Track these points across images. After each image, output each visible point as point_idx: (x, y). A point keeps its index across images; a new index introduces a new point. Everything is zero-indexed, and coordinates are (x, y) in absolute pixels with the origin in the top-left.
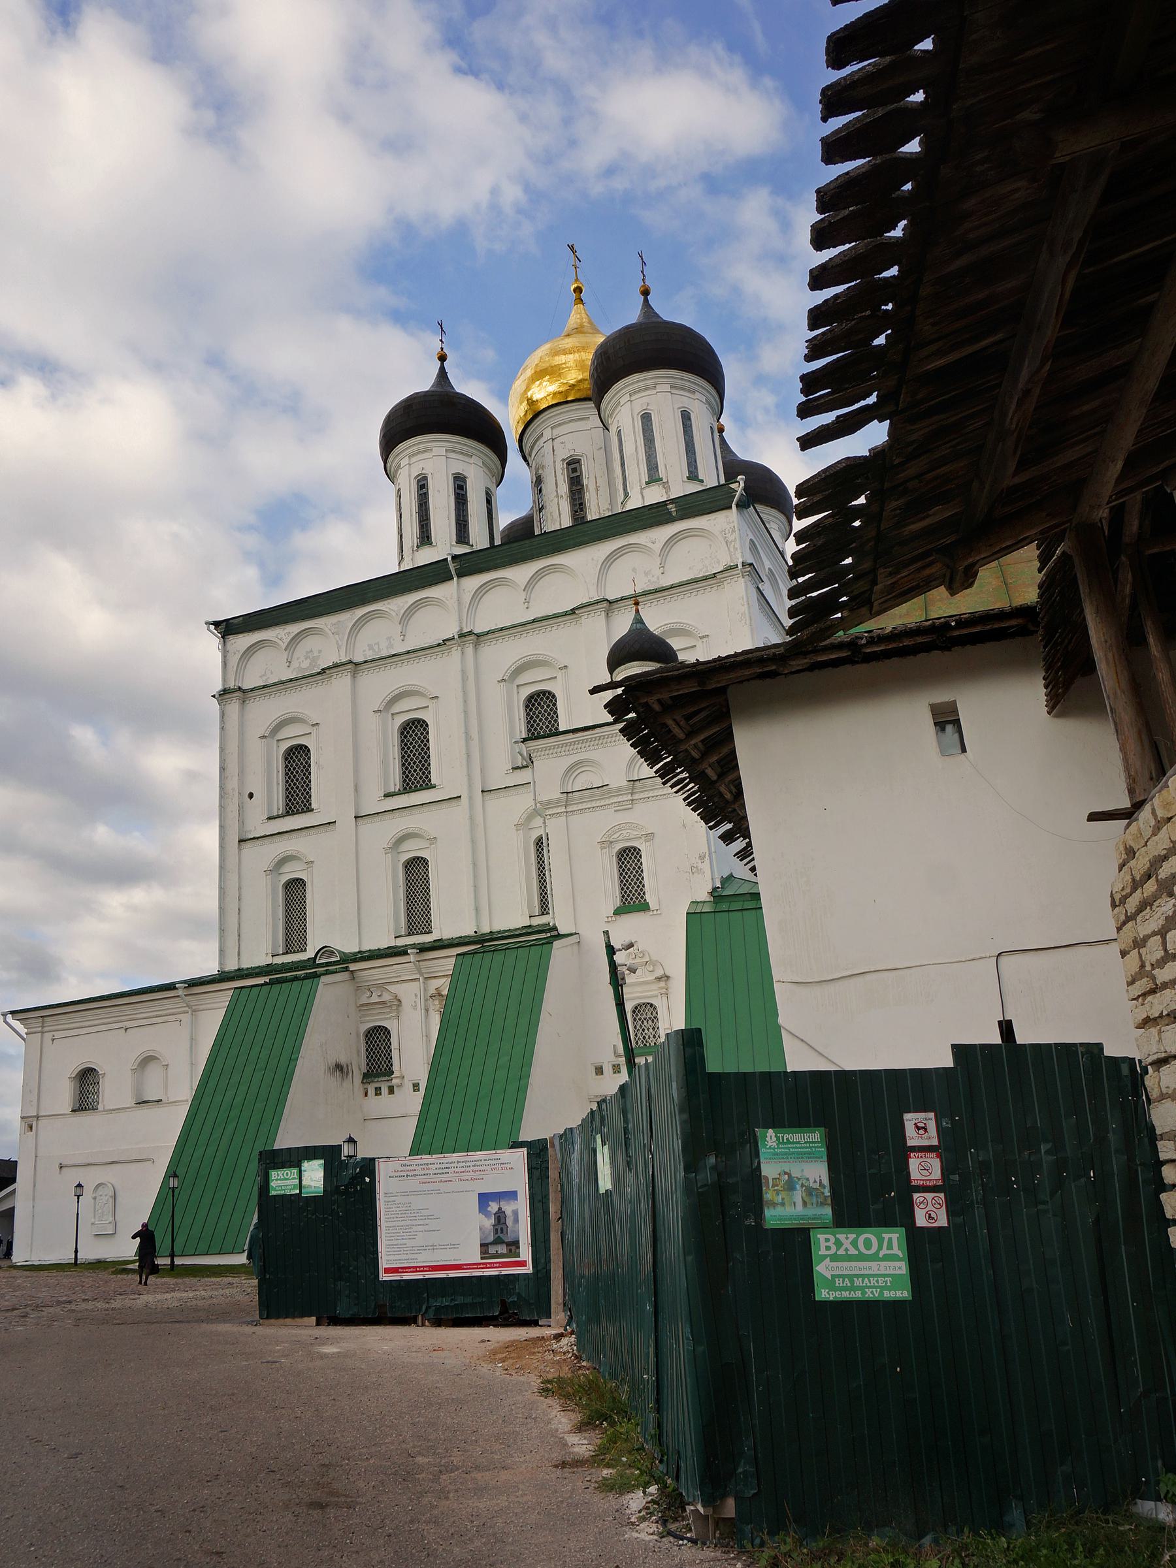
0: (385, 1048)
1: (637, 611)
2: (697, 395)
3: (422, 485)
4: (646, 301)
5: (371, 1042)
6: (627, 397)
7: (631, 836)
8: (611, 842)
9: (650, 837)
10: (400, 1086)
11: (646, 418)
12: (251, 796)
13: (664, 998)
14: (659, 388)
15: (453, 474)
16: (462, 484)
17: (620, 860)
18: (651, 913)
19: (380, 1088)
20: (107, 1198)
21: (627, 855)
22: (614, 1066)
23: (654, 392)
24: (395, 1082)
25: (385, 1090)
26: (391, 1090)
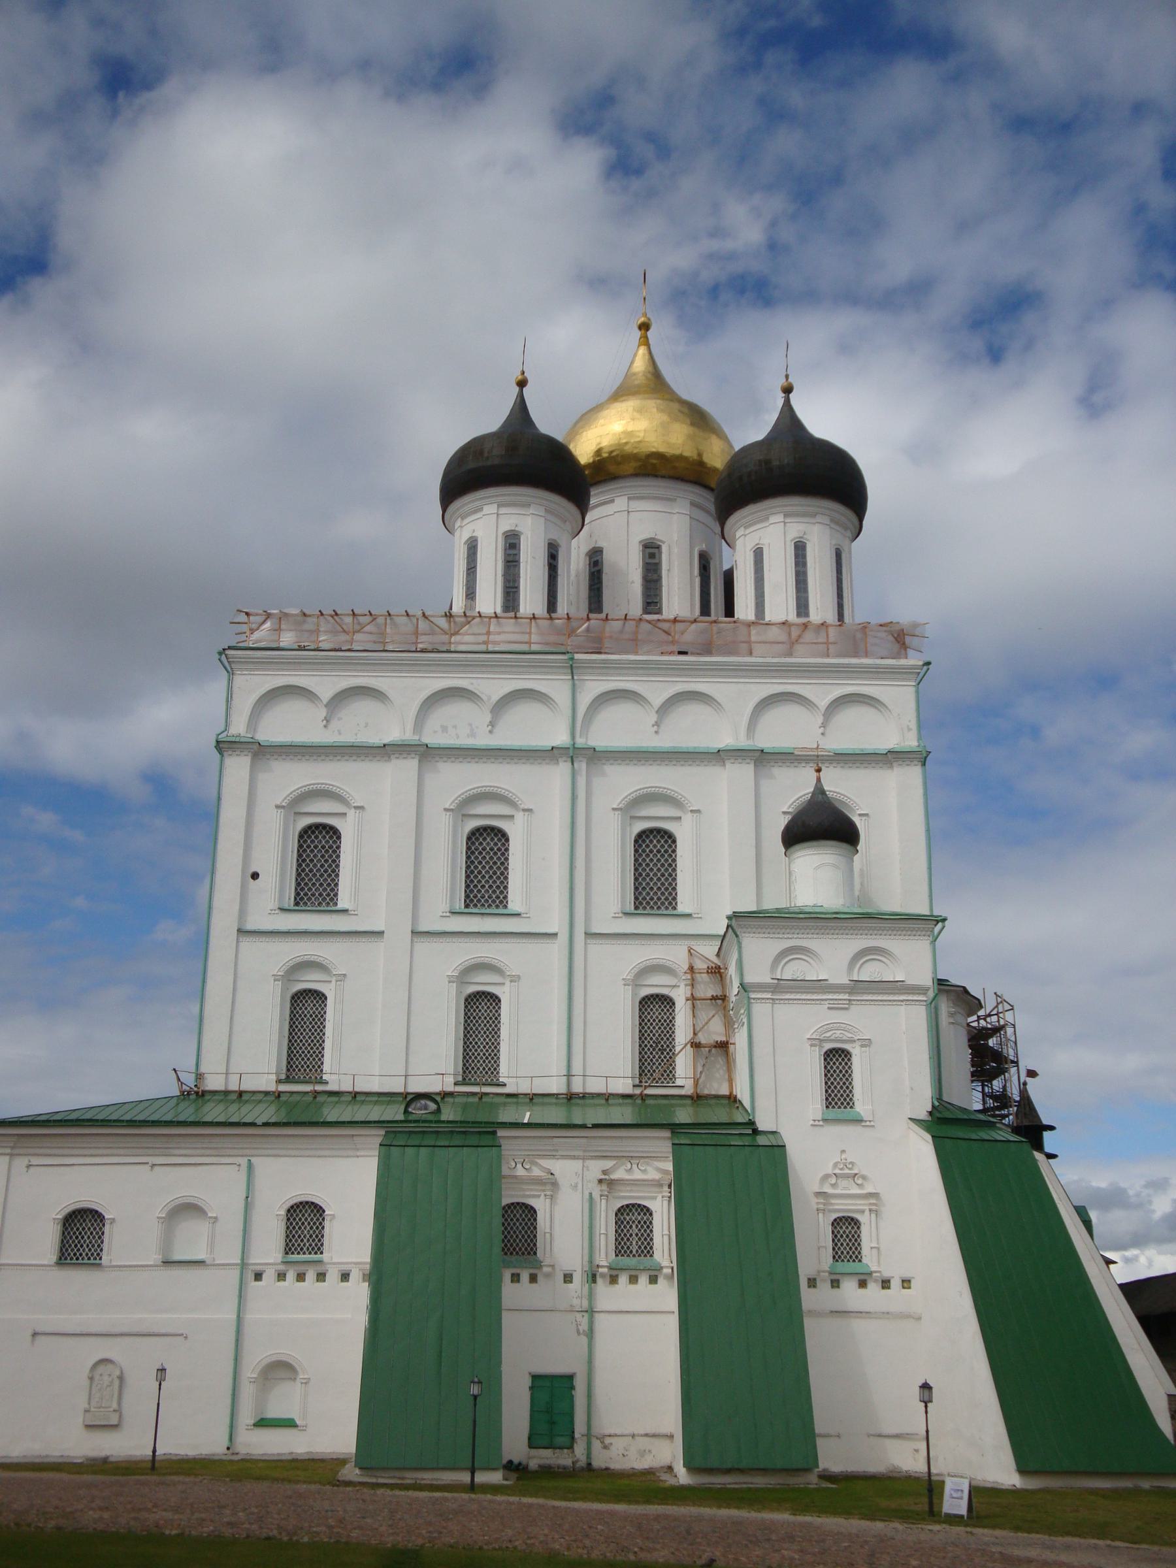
1: (819, 779)
6: (780, 518)
7: (845, 1038)
9: (866, 1043)
11: (800, 549)
12: (255, 876)
13: (873, 1216)
16: (555, 553)
17: (825, 1059)
18: (863, 1124)
19: (518, 1275)
20: (110, 1379)
21: (834, 1056)
22: (809, 1279)
24: (545, 1269)
25: (525, 1276)
26: (533, 1279)
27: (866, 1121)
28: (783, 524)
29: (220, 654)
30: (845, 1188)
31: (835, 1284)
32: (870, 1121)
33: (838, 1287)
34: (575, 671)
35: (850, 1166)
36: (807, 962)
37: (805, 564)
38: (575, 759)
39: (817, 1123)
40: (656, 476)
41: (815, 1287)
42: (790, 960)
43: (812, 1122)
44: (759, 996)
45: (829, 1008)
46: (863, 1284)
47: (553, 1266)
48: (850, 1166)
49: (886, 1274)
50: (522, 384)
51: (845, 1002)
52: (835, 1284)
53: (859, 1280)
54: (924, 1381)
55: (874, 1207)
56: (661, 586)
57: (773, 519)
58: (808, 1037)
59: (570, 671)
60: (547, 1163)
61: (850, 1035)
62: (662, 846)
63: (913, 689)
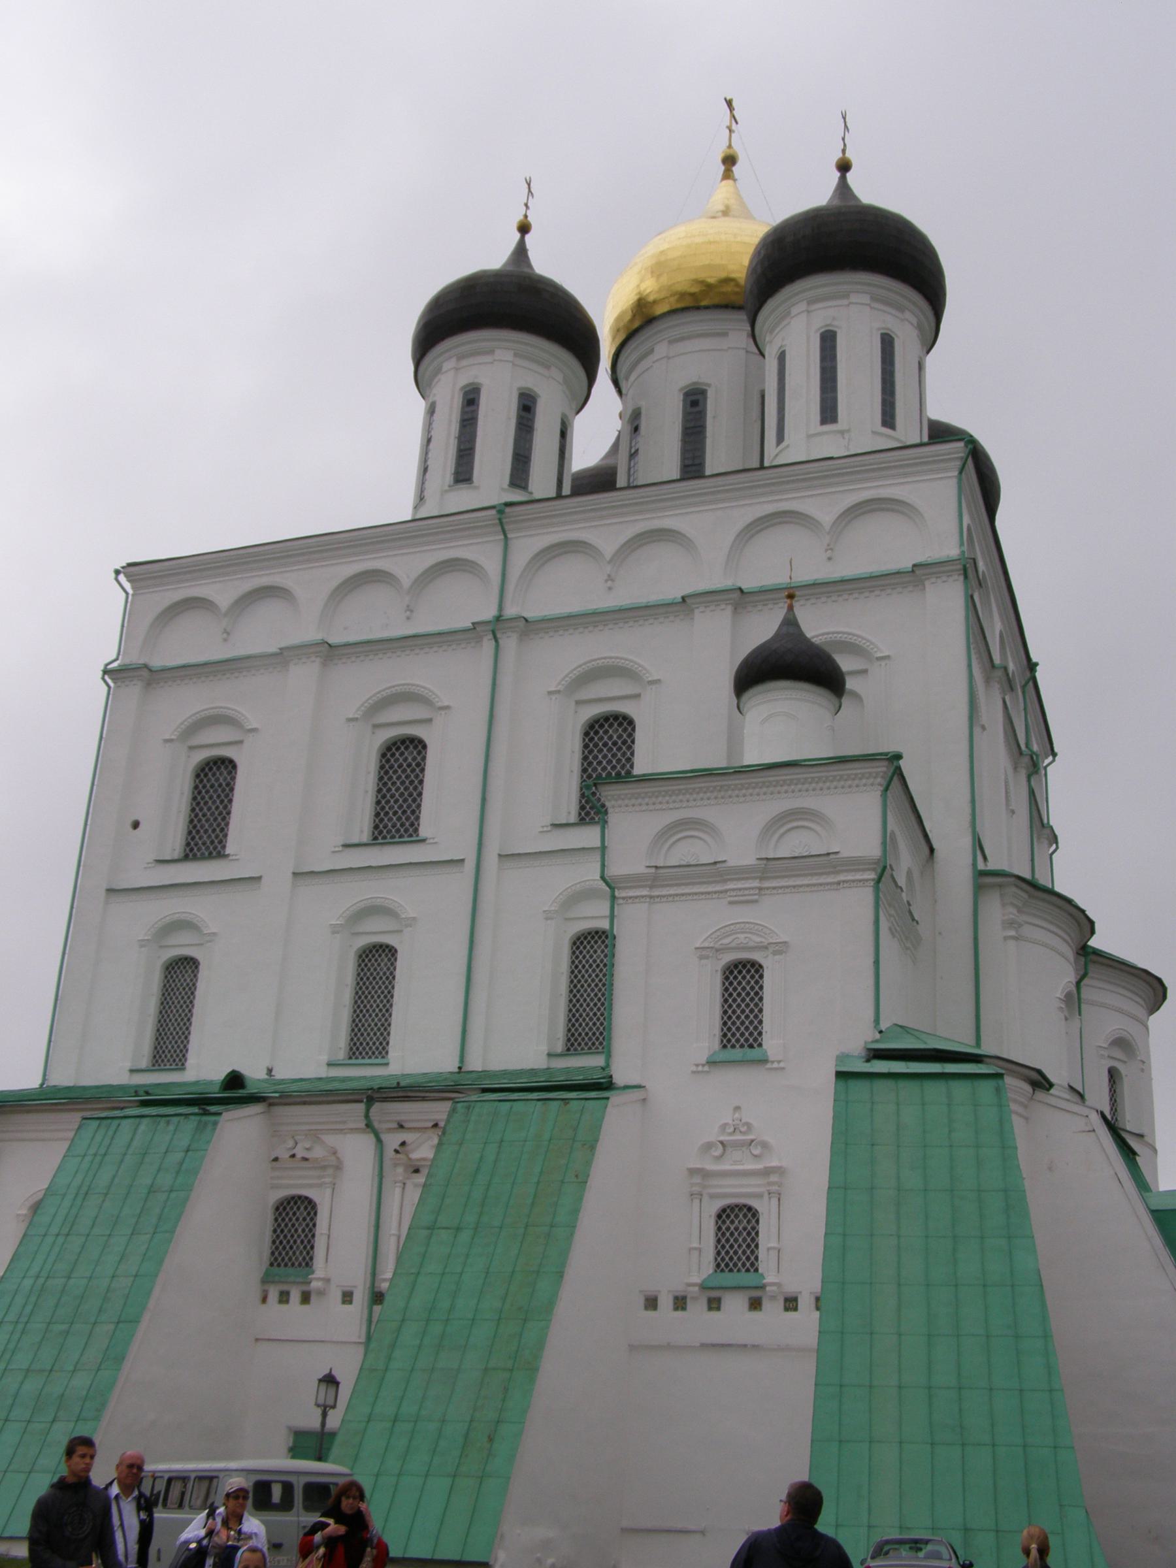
0: (303, 1231)
1: (791, 608)
2: (908, 315)
3: (471, 399)
4: (843, 179)
5: (283, 1220)
6: (803, 306)
7: (751, 944)
8: (717, 950)
9: (781, 948)
10: (321, 1293)
11: (828, 341)
12: (136, 825)
13: (774, 1201)
14: (854, 298)
15: (519, 389)
16: (529, 403)
17: (727, 978)
18: (769, 1066)
21: (740, 972)
23: (845, 302)
25: (295, 1296)
26: (306, 1298)
27: (773, 1062)
28: (805, 313)
29: (117, 572)
30: (735, 1162)
31: (714, 1305)
32: (779, 1062)
33: (718, 1309)
34: (506, 527)
35: (744, 1129)
36: (700, 839)
37: (834, 358)
38: (498, 636)
39: (700, 1068)
40: (698, 308)
41: (684, 1309)
42: (679, 840)
43: (694, 1068)
44: (631, 893)
45: (731, 903)
46: (755, 1304)
47: (327, 1280)
48: (744, 1129)
49: (791, 1288)
50: (524, 228)
51: (752, 892)
52: (714, 1304)
53: (750, 1299)
54: (327, 1371)
55: (774, 1188)
56: (705, 437)
57: (794, 311)
58: (698, 946)
59: (499, 528)
60: (330, 1140)
61: (758, 939)
62: (620, 737)
63: (955, 481)
